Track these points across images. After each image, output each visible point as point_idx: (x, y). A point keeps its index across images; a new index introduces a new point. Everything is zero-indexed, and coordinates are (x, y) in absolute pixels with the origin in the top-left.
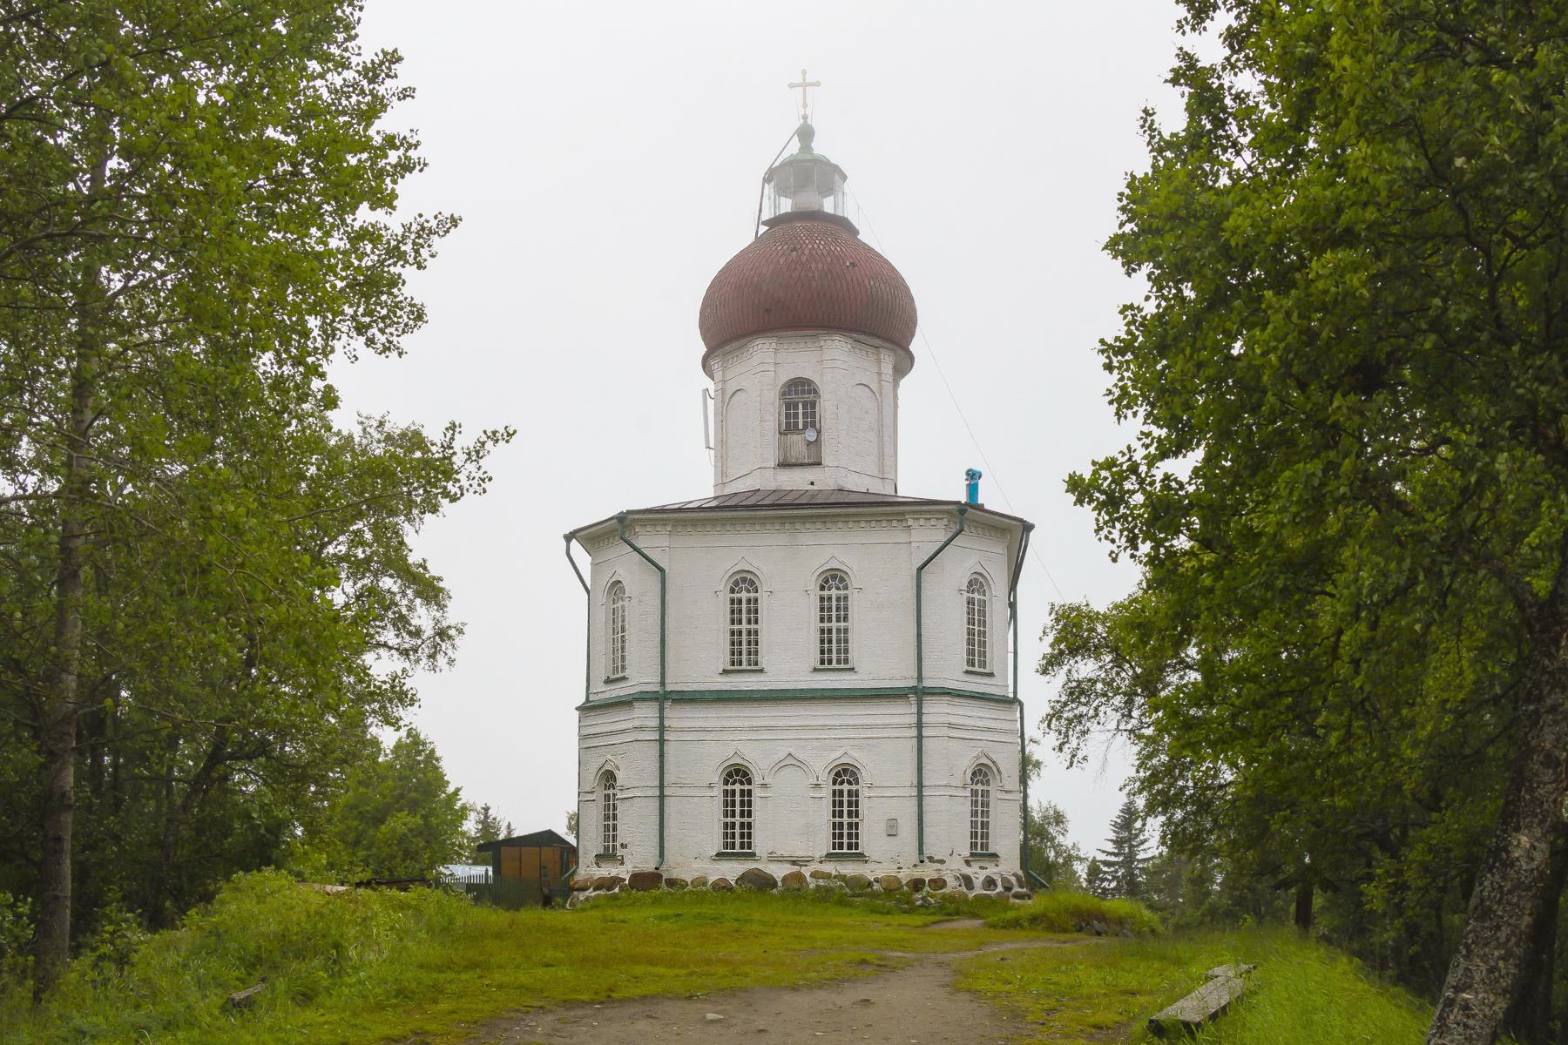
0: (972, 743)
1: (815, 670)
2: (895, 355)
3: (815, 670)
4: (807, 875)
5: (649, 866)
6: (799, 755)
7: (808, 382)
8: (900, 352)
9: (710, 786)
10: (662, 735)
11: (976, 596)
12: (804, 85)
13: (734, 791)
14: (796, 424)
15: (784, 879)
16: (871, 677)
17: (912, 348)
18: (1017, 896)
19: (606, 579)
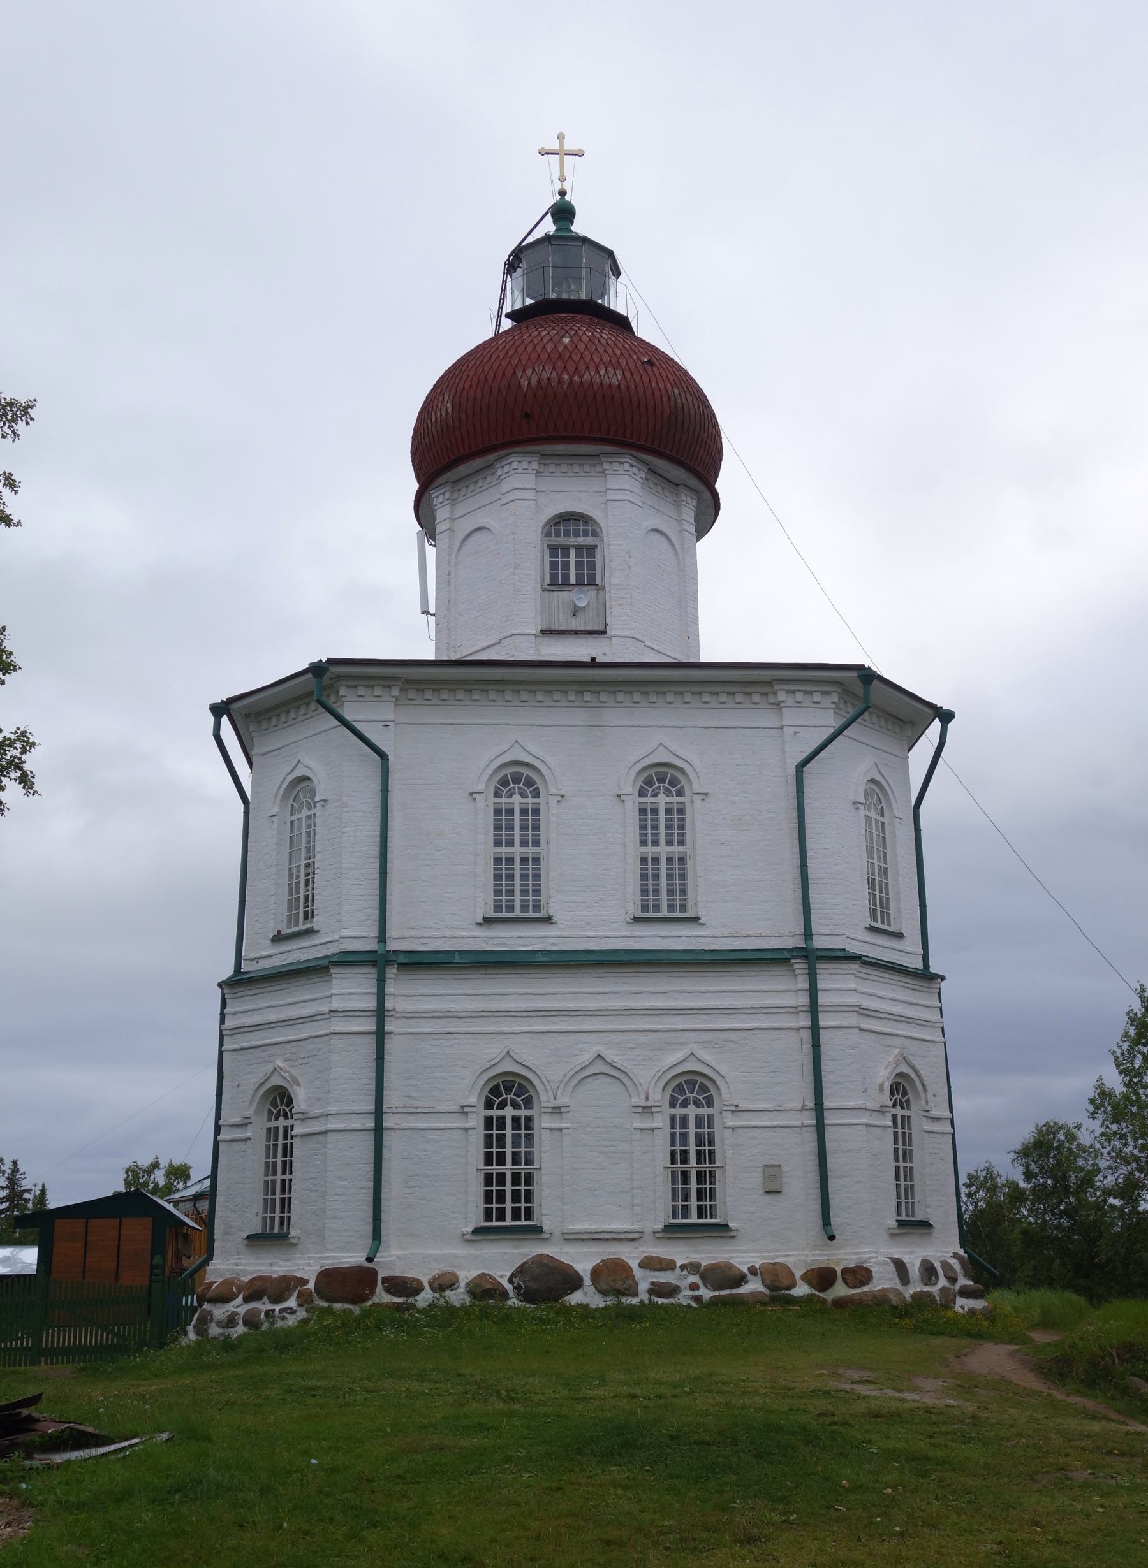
0: (888, 1040)
1: (636, 920)
2: (699, 502)
3: (636, 920)
4: (634, 1264)
5: (354, 1258)
6: (610, 1055)
8: (707, 495)
9: (463, 1111)
10: (381, 1023)
11: (873, 815)
13: (501, 1121)
14: (566, 578)
15: (596, 1273)
16: (726, 932)
17: (719, 486)
18: (965, 1293)
19: (281, 773)
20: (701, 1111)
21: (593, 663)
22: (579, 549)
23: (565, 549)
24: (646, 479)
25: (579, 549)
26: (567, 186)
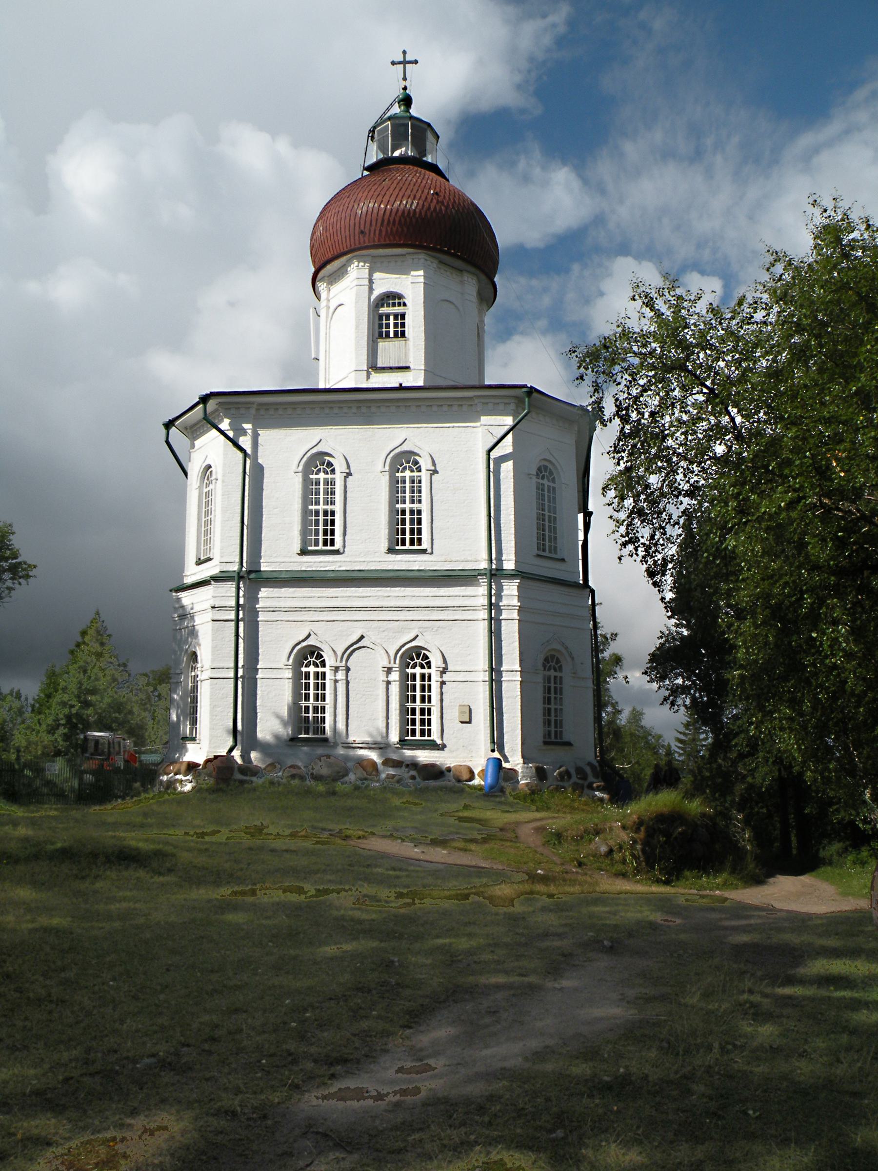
2: (479, 281)
7: (400, 296)
8: (483, 277)
12: (404, 63)
14: (388, 333)
20: (423, 671)
21: (401, 388)
22: (396, 317)
23: (388, 317)
24: (440, 268)
25: (396, 317)
26: (407, 83)
